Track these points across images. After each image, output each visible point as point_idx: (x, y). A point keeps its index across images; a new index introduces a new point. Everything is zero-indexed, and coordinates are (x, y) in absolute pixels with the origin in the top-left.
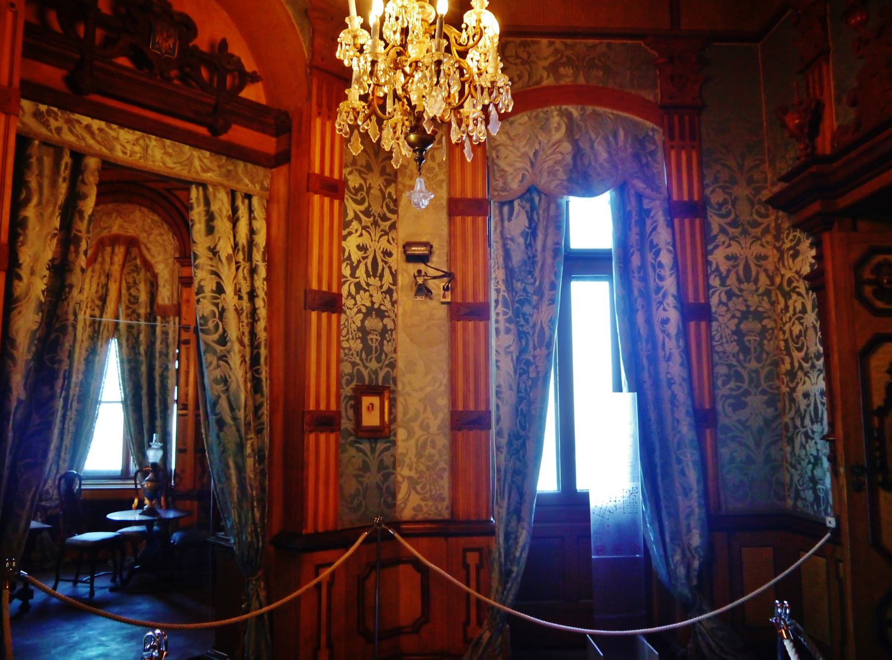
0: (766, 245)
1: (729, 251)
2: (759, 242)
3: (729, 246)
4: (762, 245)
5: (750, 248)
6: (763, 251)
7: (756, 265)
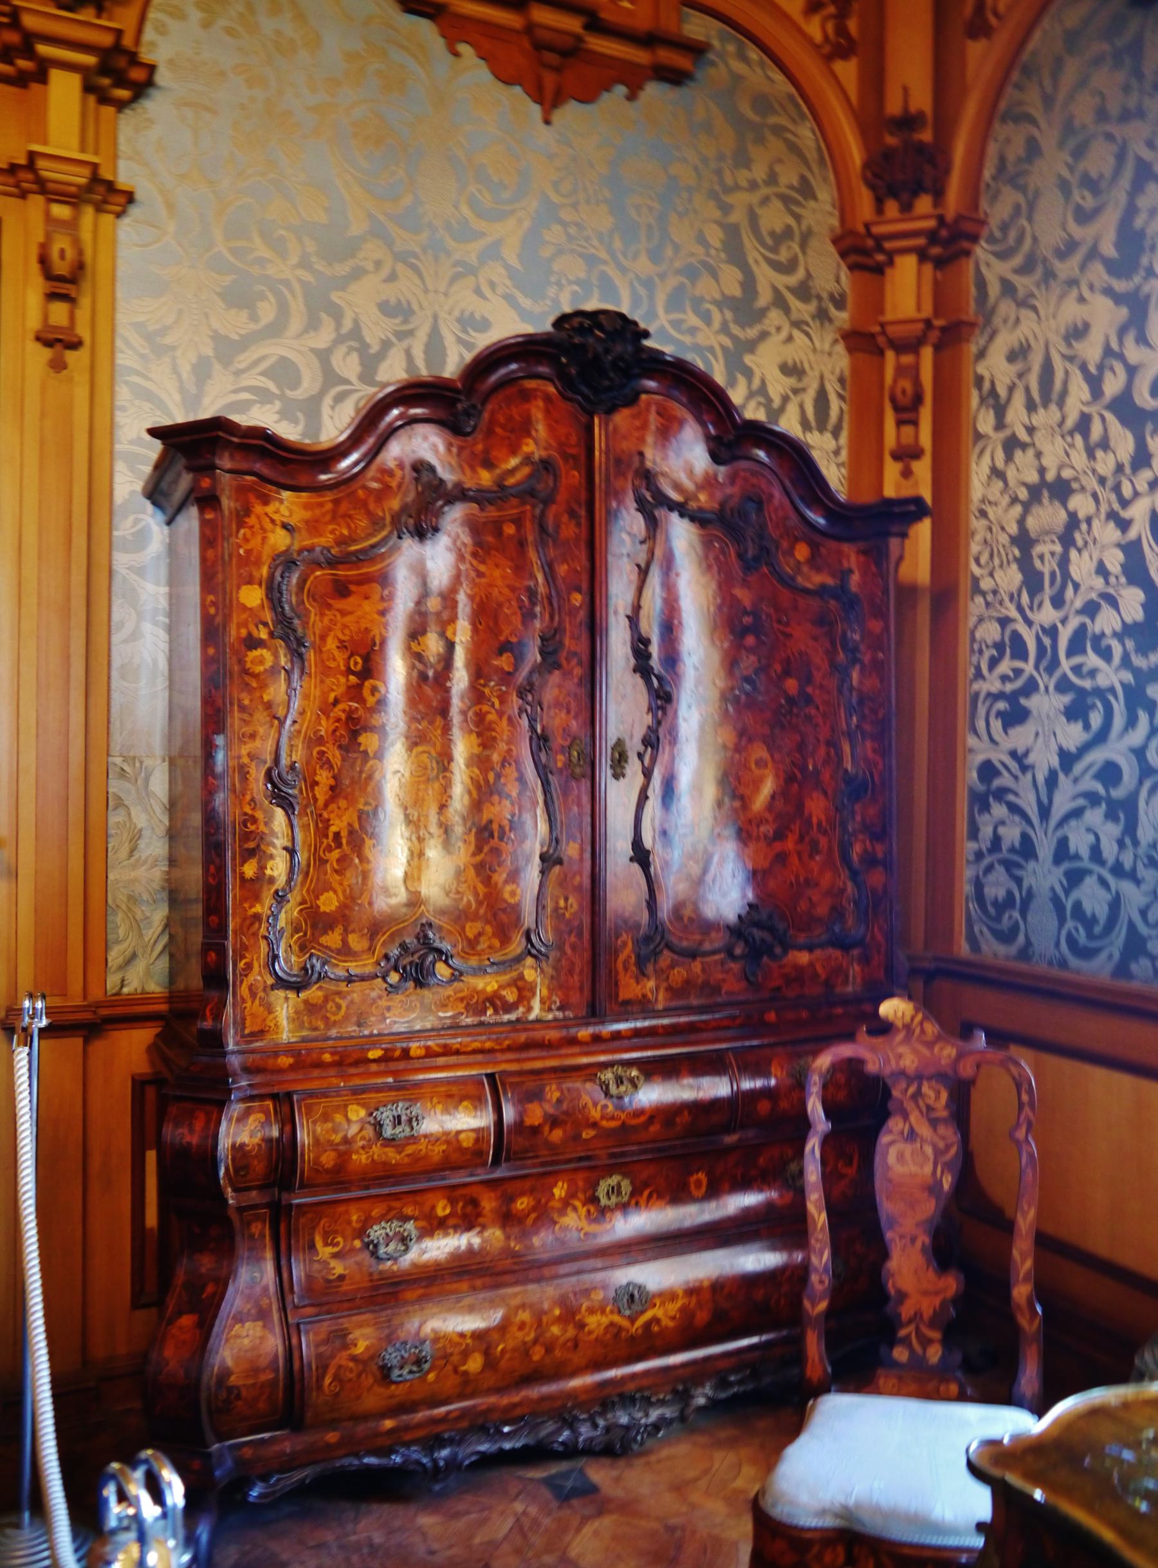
0: (486, 290)
1: (390, 293)
2: (471, 280)
3: (392, 277)
4: (478, 292)
5: (446, 294)
6: (480, 308)
7: (460, 341)
